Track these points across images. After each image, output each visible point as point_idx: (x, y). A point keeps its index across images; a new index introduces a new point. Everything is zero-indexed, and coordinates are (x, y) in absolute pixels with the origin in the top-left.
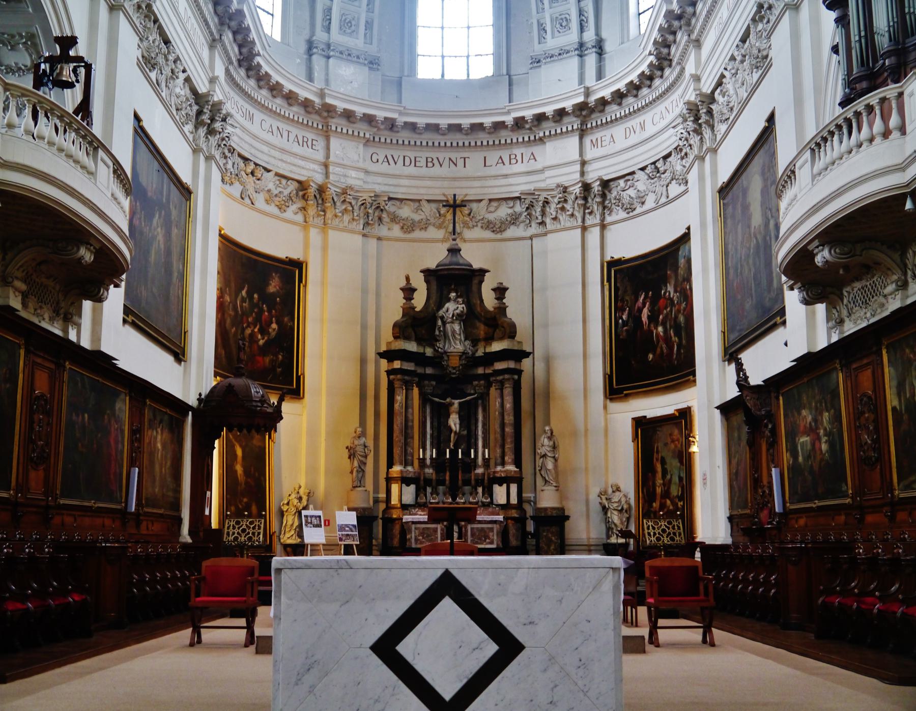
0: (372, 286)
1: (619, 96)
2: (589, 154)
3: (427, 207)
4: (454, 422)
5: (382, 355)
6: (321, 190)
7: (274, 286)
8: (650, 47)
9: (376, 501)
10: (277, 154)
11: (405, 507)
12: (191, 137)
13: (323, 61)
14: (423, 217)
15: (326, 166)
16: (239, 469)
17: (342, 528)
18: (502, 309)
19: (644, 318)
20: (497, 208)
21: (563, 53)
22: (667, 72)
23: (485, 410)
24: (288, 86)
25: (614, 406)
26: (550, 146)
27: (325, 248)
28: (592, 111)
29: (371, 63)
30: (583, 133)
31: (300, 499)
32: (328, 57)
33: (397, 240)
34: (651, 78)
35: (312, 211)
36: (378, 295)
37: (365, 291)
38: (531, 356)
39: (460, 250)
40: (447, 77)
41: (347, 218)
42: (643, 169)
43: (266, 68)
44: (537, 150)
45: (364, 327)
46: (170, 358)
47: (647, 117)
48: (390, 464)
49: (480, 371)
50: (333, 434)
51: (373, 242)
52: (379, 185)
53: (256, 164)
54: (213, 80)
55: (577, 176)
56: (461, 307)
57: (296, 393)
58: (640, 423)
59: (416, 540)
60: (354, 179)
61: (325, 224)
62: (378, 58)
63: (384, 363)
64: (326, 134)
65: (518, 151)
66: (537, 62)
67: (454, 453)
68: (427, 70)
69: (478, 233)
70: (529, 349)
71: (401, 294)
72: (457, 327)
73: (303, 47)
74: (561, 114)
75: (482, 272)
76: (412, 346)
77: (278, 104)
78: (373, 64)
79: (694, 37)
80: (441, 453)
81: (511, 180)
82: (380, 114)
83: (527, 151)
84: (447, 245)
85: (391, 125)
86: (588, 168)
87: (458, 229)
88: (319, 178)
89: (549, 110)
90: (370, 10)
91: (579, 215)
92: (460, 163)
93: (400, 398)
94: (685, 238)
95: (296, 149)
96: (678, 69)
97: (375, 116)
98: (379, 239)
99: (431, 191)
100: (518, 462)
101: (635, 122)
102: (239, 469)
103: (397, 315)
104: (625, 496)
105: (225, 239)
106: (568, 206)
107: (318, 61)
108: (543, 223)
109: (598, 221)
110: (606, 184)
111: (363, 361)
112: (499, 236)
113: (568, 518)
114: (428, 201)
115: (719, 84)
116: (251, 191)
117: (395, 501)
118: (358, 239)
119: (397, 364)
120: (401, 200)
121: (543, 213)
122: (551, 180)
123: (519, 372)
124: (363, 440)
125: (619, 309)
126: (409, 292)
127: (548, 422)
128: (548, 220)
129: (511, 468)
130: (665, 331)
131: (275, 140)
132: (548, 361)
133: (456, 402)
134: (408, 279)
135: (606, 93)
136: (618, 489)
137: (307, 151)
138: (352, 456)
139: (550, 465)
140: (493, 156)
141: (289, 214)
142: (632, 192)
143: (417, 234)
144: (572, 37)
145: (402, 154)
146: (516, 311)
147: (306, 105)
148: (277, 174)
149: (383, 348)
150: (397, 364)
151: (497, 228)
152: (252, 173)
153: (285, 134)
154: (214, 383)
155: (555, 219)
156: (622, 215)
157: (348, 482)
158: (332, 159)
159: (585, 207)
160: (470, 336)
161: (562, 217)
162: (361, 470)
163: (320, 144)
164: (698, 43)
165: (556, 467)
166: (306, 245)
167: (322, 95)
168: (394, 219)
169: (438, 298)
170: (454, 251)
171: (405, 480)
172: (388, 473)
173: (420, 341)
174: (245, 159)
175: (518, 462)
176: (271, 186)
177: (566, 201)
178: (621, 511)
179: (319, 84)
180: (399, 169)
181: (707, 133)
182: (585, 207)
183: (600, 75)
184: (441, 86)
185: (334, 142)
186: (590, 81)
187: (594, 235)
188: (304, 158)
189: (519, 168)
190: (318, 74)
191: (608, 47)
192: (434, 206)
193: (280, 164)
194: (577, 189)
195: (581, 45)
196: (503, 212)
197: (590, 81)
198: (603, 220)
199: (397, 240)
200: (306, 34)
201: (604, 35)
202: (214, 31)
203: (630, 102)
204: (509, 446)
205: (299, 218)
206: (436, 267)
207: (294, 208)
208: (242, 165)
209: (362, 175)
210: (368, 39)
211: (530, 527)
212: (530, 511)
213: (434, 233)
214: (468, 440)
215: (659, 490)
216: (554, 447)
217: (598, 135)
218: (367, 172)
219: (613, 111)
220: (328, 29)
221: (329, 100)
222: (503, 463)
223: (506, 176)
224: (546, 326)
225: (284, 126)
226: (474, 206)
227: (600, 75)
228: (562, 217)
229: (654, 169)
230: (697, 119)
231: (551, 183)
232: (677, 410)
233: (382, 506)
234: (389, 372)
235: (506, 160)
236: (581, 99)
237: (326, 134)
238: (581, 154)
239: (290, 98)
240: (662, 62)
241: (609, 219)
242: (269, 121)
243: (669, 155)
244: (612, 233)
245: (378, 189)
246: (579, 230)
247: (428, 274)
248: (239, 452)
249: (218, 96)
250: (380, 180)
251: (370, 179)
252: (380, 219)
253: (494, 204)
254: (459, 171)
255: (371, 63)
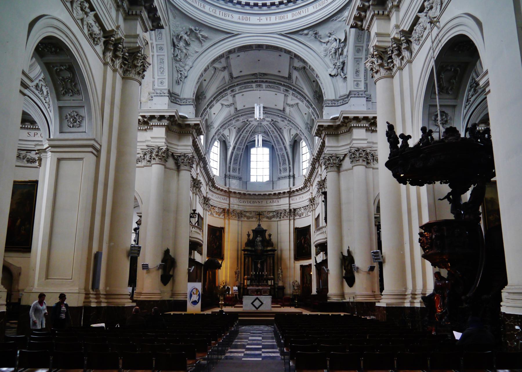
0: (240, 233)
1: (297, 190)
2: (291, 203)
3: (253, 213)
4: (259, 266)
5: (243, 250)
6: (228, 210)
7: (218, 234)
8: (303, 183)
9: (241, 284)
10: (218, 203)
11: (248, 286)
12: (203, 206)
13: (228, 179)
14: (252, 215)
15: (229, 204)
16: (211, 277)
17: (235, 290)
18: (270, 240)
19: (303, 242)
20: (269, 213)
21: (285, 177)
22: (307, 188)
23: (266, 263)
24: (221, 188)
25: (296, 262)
26: (282, 199)
27: (229, 224)
28: (291, 193)
29: (240, 178)
30: (290, 197)
31: (224, 283)
32: (230, 178)
33: (246, 221)
34: (304, 188)
35: (226, 216)
36: (241, 235)
37: (238, 234)
38: (277, 251)
39: (260, 225)
40: (258, 181)
41: (234, 217)
42: (303, 207)
43: (217, 185)
44: (279, 200)
45: (238, 242)
46: (200, 255)
47: (304, 195)
48: (244, 275)
49: (265, 254)
50: (231, 268)
51: (240, 222)
52: (241, 208)
53: (214, 206)
54: (207, 193)
55: (288, 207)
56: (261, 239)
57: (222, 259)
58: (302, 266)
59: (251, 293)
60: (236, 207)
61: (229, 218)
62: (241, 177)
63: (243, 252)
64: (229, 197)
65: (274, 200)
66: (279, 179)
67: (259, 273)
68: (253, 179)
69: (265, 219)
70: (276, 249)
71: (247, 236)
72: (260, 243)
73: (224, 176)
74: (284, 193)
75: (266, 230)
76: (249, 248)
77: (218, 192)
78: (240, 179)
79: (311, 184)
80: (256, 273)
81: (273, 207)
82: (242, 192)
83: (277, 200)
84: (258, 223)
85: (244, 194)
86: (291, 205)
87: (260, 218)
88: (228, 208)
89: (282, 192)
90: (239, 166)
91: (289, 217)
92: (261, 202)
93: (247, 260)
94: (310, 225)
95: (223, 201)
96: (309, 189)
97: (241, 193)
98: (242, 221)
99: (254, 209)
100: (274, 275)
101: (301, 196)
102: (211, 277)
103: (246, 240)
104: (298, 283)
105: (208, 225)
106: (286, 214)
107: (227, 179)
108: (280, 218)
109: (293, 218)
110: (295, 210)
111: (238, 251)
112: (270, 220)
113: (285, 288)
114: (253, 212)
115: (315, 197)
116: (213, 212)
117: (245, 284)
118: (237, 221)
119: (246, 253)
120: (247, 211)
121: (280, 215)
122: (282, 208)
123: (274, 254)
124: (238, 270)
125: (297, 239)
126: (249, 235)
127: (281, 266)
128: (281, 217)
129: (272, 276)
130: (307, 246)
131: (218, 200)
132: (281, 251)
133: (260, 261)
134: (248, 232)
135: (295, 189)
136: (297, 281)
137: (225, 201)
138: (236, 273)
139: (281, 276)
140: (269, 201)
141: (221, 217)
142: (300, 212)
143: (250, 220)
144: (287, 174)
145: (247, 200)
146: (274, 239)
147: (225, 191)
148: (218, 208)
149: (243, 249)
150: (246, 253)
151: (270, 218)
152: (213, 209)
153: (220, 198)
154: (207, 259)
155: (283, 217)
156: (298, 217)
157: (235, 279)
158: (231, 203)
159: (290, 215)
160: (263, 245)
161: (285, 217)
162: (238, 277)
163: (228, 199)
164: (312, 185)
165: (282, 276)
166: (225, 224)
167: (229, 189)
168: (245, 216)
169: (255, 237)
170: (259, 225)
171: (248, 279)
172: (244, 277)
173: (251, 247)
174: (212, 206)
175: (274, 275)
176: (217, 211)
177: (285, 213)
178: (297, 286)
179: (227, 186)
180: (245, 204)
181: (313, 205)
182: (290, 215)
183: (294, 185)
184: (257, 183)
185: (231, 199)
186: (291, 186)
187: (292, 221)
188: (224, 203)
189: (275, 204)
190: (227, 183)
191: (296, 176)
192: (254, 213)
193: (219, 205)
194: (288, 211)
195: (290, 176)
196: (271, 214)
197: (291, 186)
198: (294, 218)
199: (246, 221)
200: (224, 173)
201: (295, 174)
202: (197, 162)
203: (300, 192)
204: (272, 271)
205: (223, 217)
206: (256, 229)
207: (222, 215)
208: (211, 207)
209: (237, 206)
210: (239, 173)
211: (276, 290)
212: (276, 286)
213: (254, 219)
214: (262, 270)
215: (305, 282)
216: (282, 272)
217: (293, 198)
218: (239, 205)
219: (296, 193)
220: (229, 171)
221: (230, 190)
222: (270, 276)
223: (272, 206)
224: (281, 242)
225: (220, 196)
226: (264, 213)
227: (294, 185)
228: (285, 217)
229: (305, 208)
230: (312, 202)
231: (282, 208)
232: (309, 264)
233: (242, 285)
234: (244, 254)
235: (272, 202)
236: (289, 190)
237: (229, 197)
238: (289, 202)
239: (222, 190)
240: (305, 186)
241: (295, 218)
242: (217, 196)
243: (308, 205)
244: (296, 221)
245: (241, 209)
246: (288, 220)
247: (253, 231)
248: (211, 273)
249: (208, 196)
250: (242, 207)
251: (240, 207)
252: (242, 216)
253: (269, 212)
254: (261, 204)
255: (240, 178)
